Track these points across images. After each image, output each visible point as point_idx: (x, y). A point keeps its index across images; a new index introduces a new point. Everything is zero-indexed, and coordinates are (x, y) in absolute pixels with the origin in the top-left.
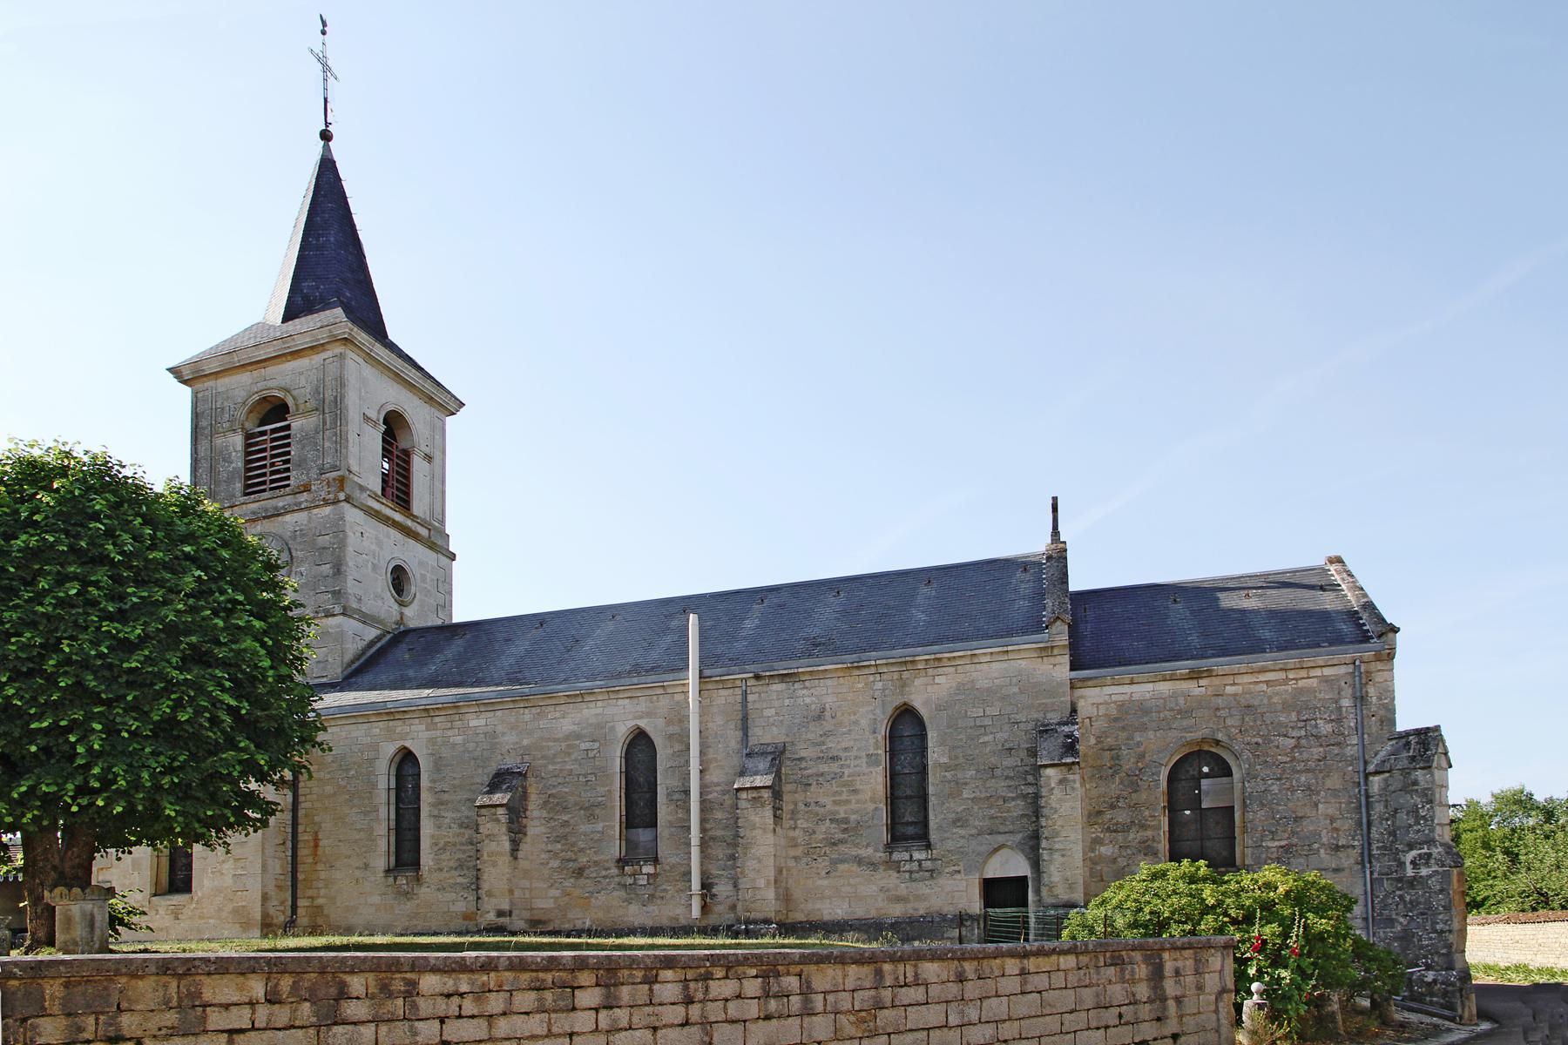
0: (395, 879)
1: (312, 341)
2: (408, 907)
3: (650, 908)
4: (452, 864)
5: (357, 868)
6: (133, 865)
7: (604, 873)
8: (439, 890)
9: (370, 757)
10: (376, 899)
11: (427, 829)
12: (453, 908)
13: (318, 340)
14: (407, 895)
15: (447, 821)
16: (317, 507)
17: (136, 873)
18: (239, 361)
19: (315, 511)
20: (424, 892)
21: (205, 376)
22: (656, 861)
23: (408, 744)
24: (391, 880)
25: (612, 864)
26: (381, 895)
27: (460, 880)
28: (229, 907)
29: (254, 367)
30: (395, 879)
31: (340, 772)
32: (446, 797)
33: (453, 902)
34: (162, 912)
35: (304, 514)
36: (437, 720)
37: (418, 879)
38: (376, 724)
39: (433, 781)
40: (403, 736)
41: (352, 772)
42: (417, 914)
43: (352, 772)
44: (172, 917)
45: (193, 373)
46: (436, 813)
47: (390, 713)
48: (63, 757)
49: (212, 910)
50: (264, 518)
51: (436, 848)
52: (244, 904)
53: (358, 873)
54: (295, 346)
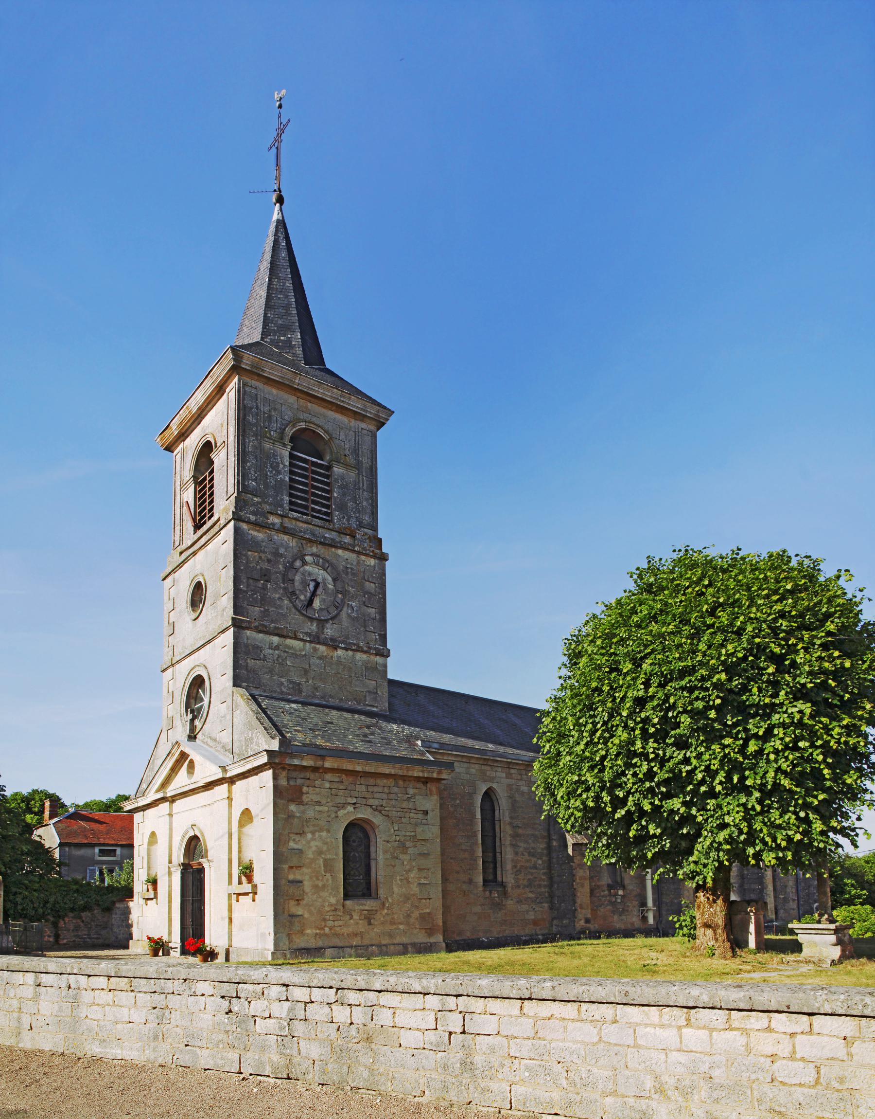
0: (491, 893)
1: (362, 409)
2: (499, 915)
3: (623, 917)
4: (525, 882)
5: (464, 882)
6: (325, 865)
7: (602, 894)
8: (518, 902)
9: (470, 791)
10: (477, 909)
11: (508, 854)
12: (527, 917)
13: (367, 411)
14: (498, 906)
15: (521, 849)
16: (367, 555)
17: (328, 875)
18: (299, 384)
19: (363, 558)
20: (510, 903)
21: (259, 375)
22: (623, 887)
23: (495, 786)
24: (488, 893)
25: (605, 888)
26: (481, 905)
27: (530, 895)
28: (416, 914)
29: (305, 397)
30: (491, 893)
31: (449, 800)
32: (520, 831)
33: (527, 911)
34: (356, 917)
35: (353, 556)
36: (512, 771)
37: (505, 894)
38: (473, 766)
39: (511, 818)
40: (492, 779)
41: (458, 802)
42: (505, 921)
43: (458, 802)
44: (365, 922)
45: (252, 366)
46: (514, 842)
47: (487, 760)
48: (702, 761)
49: (401, 916)
50: (321, 543)
51: (515, 870)
52: (428, 911)
53: (465, 887)
54: (348, 404)
